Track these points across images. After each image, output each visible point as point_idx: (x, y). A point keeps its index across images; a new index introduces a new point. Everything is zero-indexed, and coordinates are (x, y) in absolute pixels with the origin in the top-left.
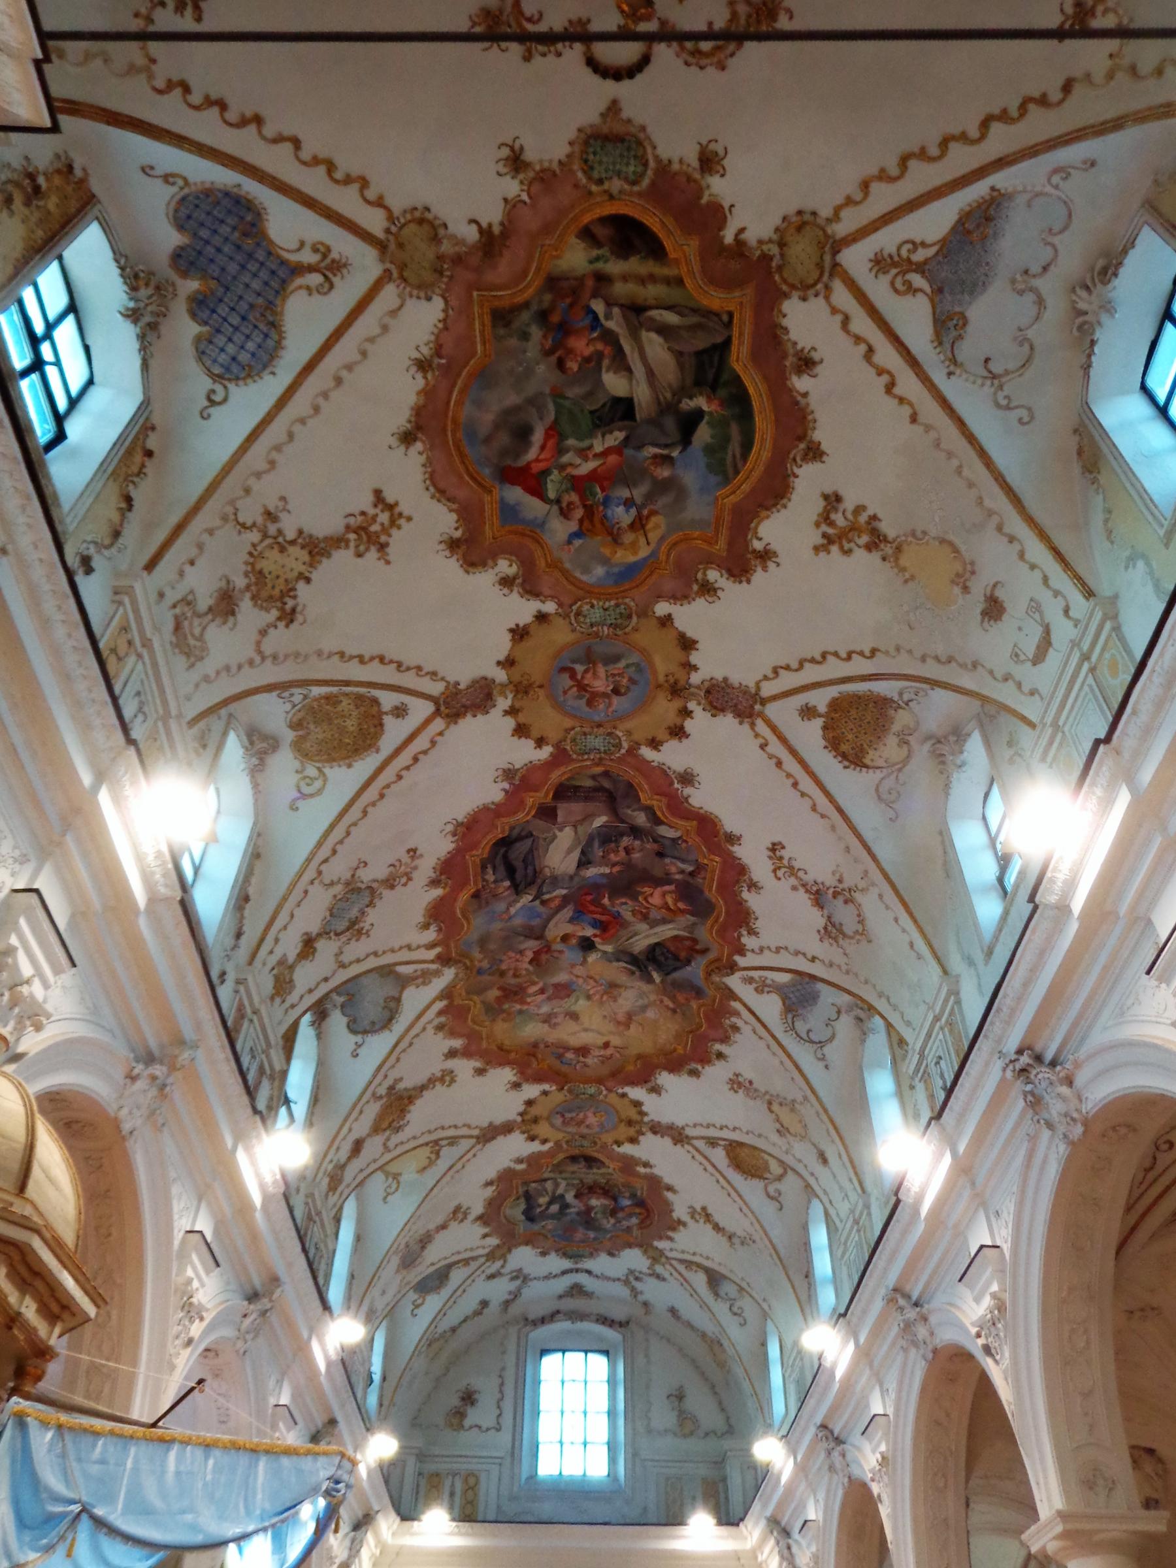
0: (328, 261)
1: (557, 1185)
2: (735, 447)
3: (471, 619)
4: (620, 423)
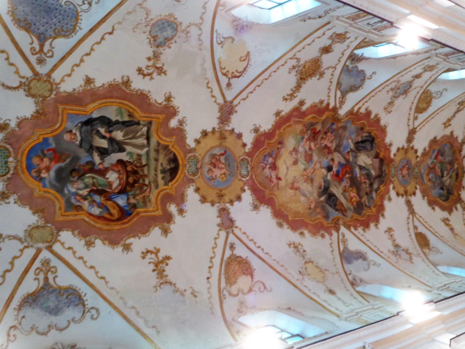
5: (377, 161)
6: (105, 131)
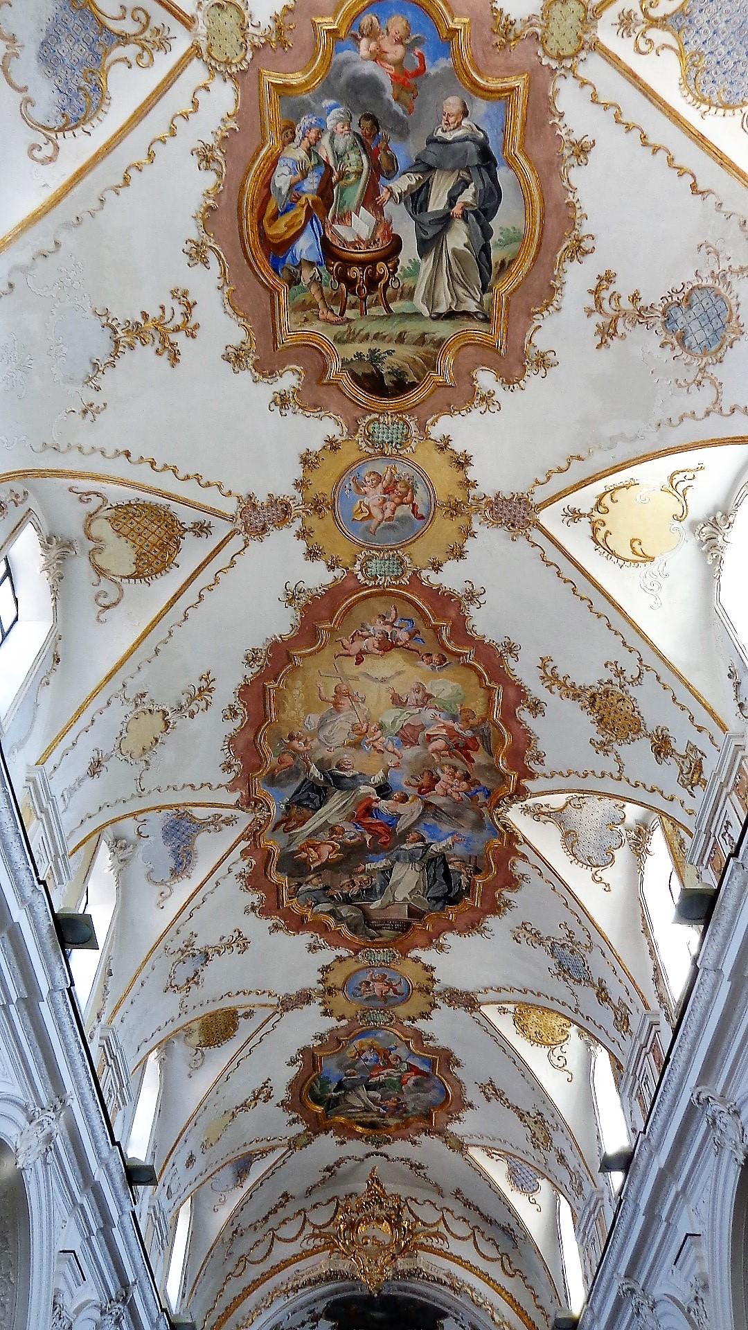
5: (404, 915)
6: (466, 204)
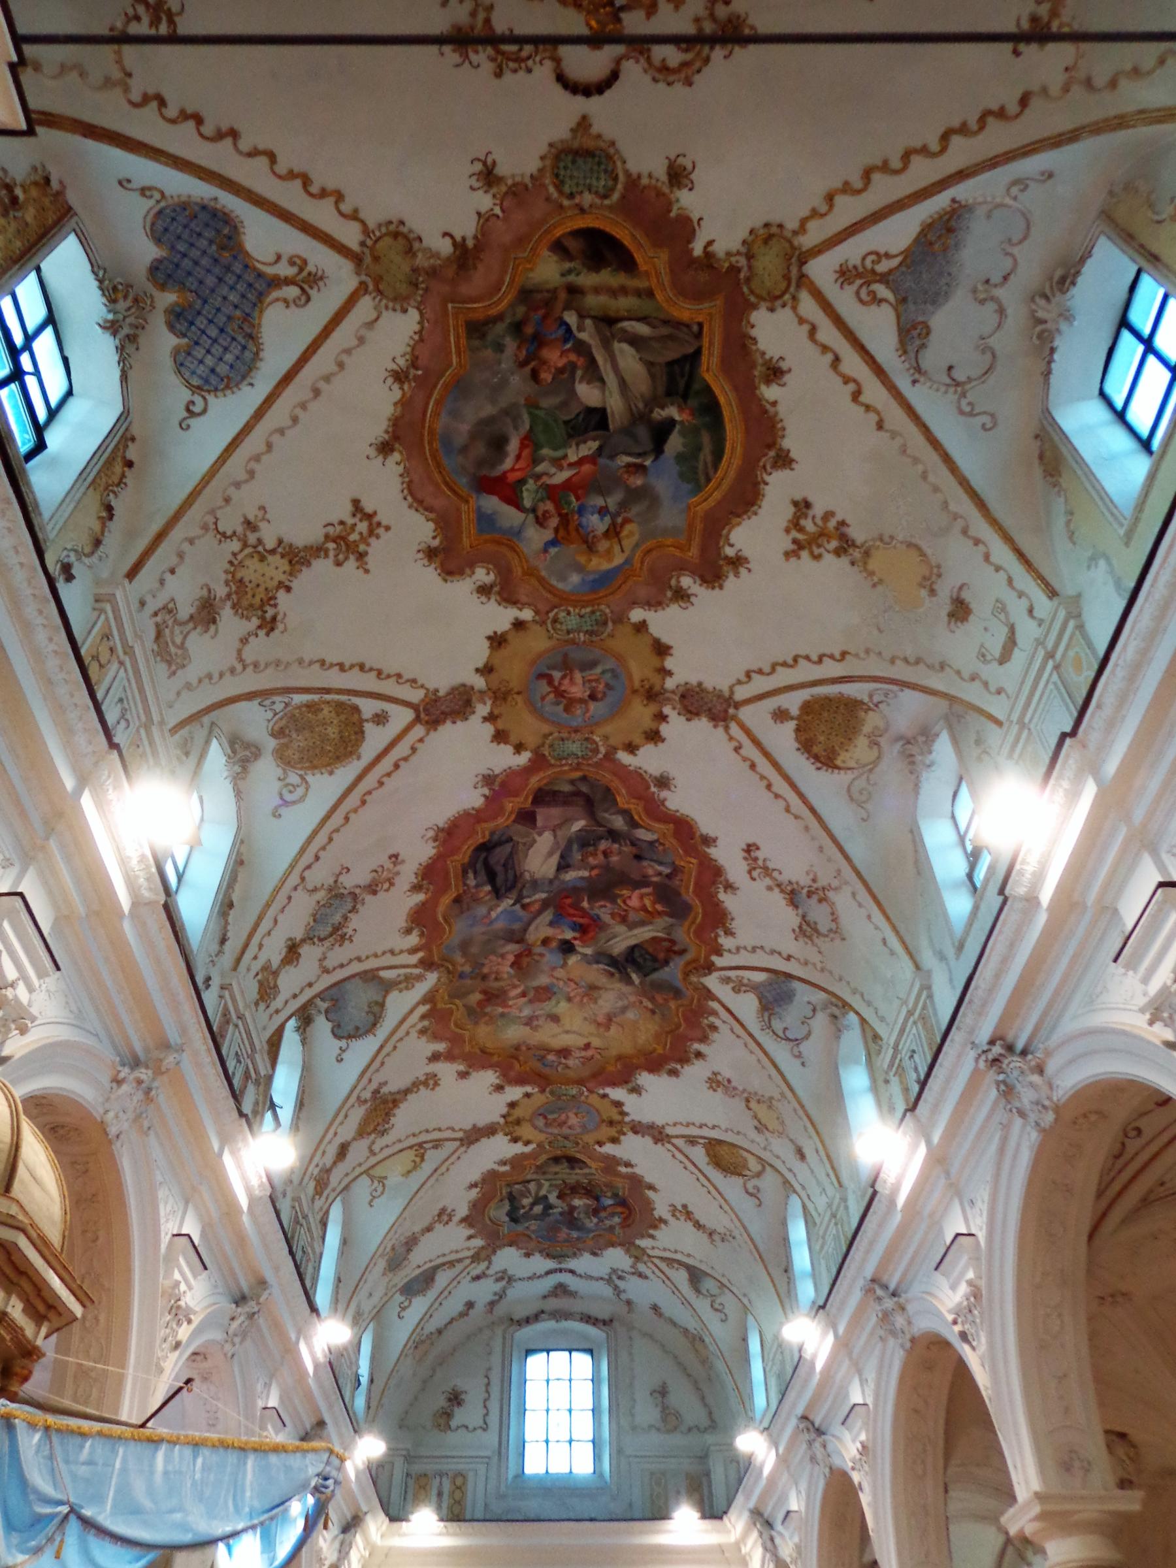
0: (305, 274)
1: (540, 1186)
2: (706, 454)
3: (450, 627)
4: (592, 434)
5: (542, 815)
